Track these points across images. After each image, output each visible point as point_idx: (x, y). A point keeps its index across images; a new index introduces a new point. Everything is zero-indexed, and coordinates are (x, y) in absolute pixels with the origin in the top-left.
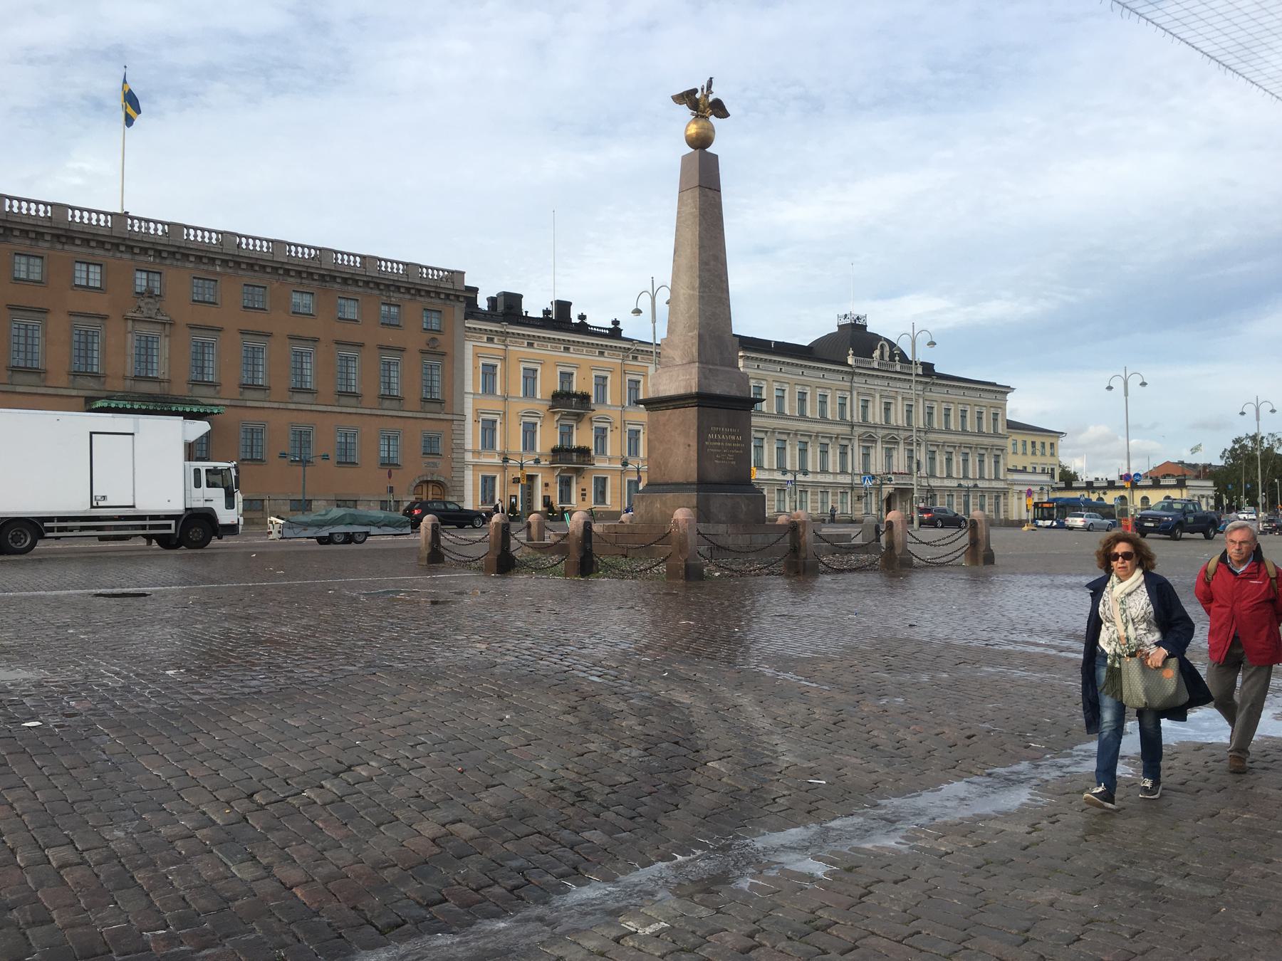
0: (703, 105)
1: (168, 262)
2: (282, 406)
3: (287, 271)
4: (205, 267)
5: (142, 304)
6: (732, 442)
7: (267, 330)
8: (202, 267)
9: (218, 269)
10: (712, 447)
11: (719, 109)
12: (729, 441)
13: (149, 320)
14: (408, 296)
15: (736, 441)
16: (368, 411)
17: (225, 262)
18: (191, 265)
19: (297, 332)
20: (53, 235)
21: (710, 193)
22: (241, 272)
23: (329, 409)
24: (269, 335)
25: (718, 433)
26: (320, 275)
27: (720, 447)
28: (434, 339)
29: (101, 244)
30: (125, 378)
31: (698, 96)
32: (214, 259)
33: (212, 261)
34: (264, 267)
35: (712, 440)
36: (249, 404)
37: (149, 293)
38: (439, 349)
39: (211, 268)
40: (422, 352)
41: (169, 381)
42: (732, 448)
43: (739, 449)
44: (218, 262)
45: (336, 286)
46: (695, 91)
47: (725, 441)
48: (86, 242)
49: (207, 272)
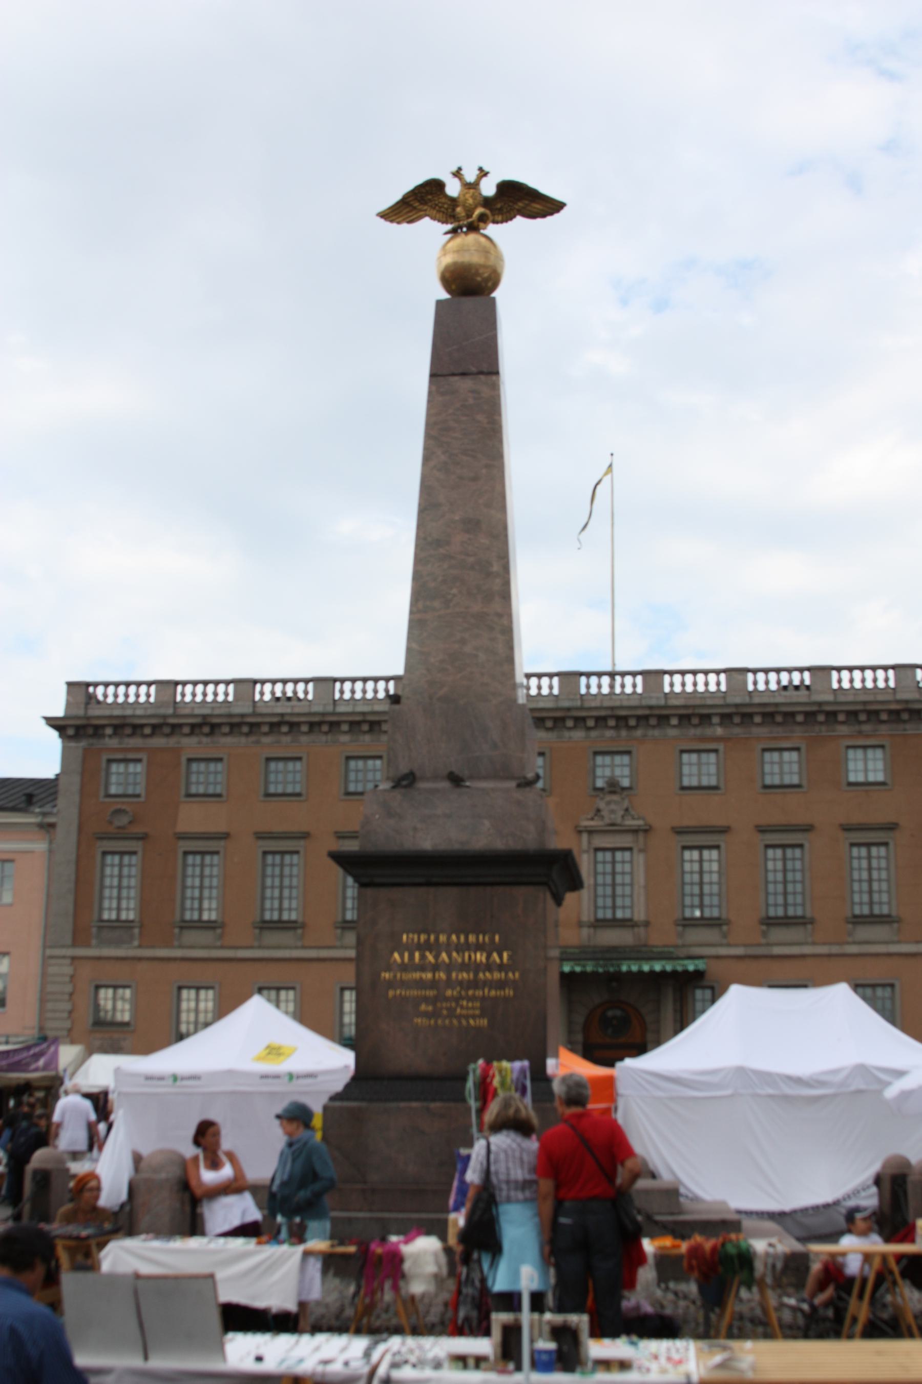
0: (477, 210)
1: (639, 733)
2: (835, 949)
4: (698, 731)
5: (602, 805)
6: (477, 968)
8: (692, 732)
9: (719, 731)
10: (404, 984)
12: (464, 967)
13: (613, 829)
15: (489, 967)
17: (726, 718)
19: (857, 818)
21: (464, 384)
24: (808, 829)
25: (424, 947)
26: (890, 712)
27: (433, 984)
30: (580, 924)
31: (453, 189)
33: (705, 719)
35: (404, 968)
36: (777, 950)
39: (708, 731)
41: (647, 924)
42: (475, 984)
43: (501, 985)
44: (716, 720)
46: (434, 187)
47: (449, 968)
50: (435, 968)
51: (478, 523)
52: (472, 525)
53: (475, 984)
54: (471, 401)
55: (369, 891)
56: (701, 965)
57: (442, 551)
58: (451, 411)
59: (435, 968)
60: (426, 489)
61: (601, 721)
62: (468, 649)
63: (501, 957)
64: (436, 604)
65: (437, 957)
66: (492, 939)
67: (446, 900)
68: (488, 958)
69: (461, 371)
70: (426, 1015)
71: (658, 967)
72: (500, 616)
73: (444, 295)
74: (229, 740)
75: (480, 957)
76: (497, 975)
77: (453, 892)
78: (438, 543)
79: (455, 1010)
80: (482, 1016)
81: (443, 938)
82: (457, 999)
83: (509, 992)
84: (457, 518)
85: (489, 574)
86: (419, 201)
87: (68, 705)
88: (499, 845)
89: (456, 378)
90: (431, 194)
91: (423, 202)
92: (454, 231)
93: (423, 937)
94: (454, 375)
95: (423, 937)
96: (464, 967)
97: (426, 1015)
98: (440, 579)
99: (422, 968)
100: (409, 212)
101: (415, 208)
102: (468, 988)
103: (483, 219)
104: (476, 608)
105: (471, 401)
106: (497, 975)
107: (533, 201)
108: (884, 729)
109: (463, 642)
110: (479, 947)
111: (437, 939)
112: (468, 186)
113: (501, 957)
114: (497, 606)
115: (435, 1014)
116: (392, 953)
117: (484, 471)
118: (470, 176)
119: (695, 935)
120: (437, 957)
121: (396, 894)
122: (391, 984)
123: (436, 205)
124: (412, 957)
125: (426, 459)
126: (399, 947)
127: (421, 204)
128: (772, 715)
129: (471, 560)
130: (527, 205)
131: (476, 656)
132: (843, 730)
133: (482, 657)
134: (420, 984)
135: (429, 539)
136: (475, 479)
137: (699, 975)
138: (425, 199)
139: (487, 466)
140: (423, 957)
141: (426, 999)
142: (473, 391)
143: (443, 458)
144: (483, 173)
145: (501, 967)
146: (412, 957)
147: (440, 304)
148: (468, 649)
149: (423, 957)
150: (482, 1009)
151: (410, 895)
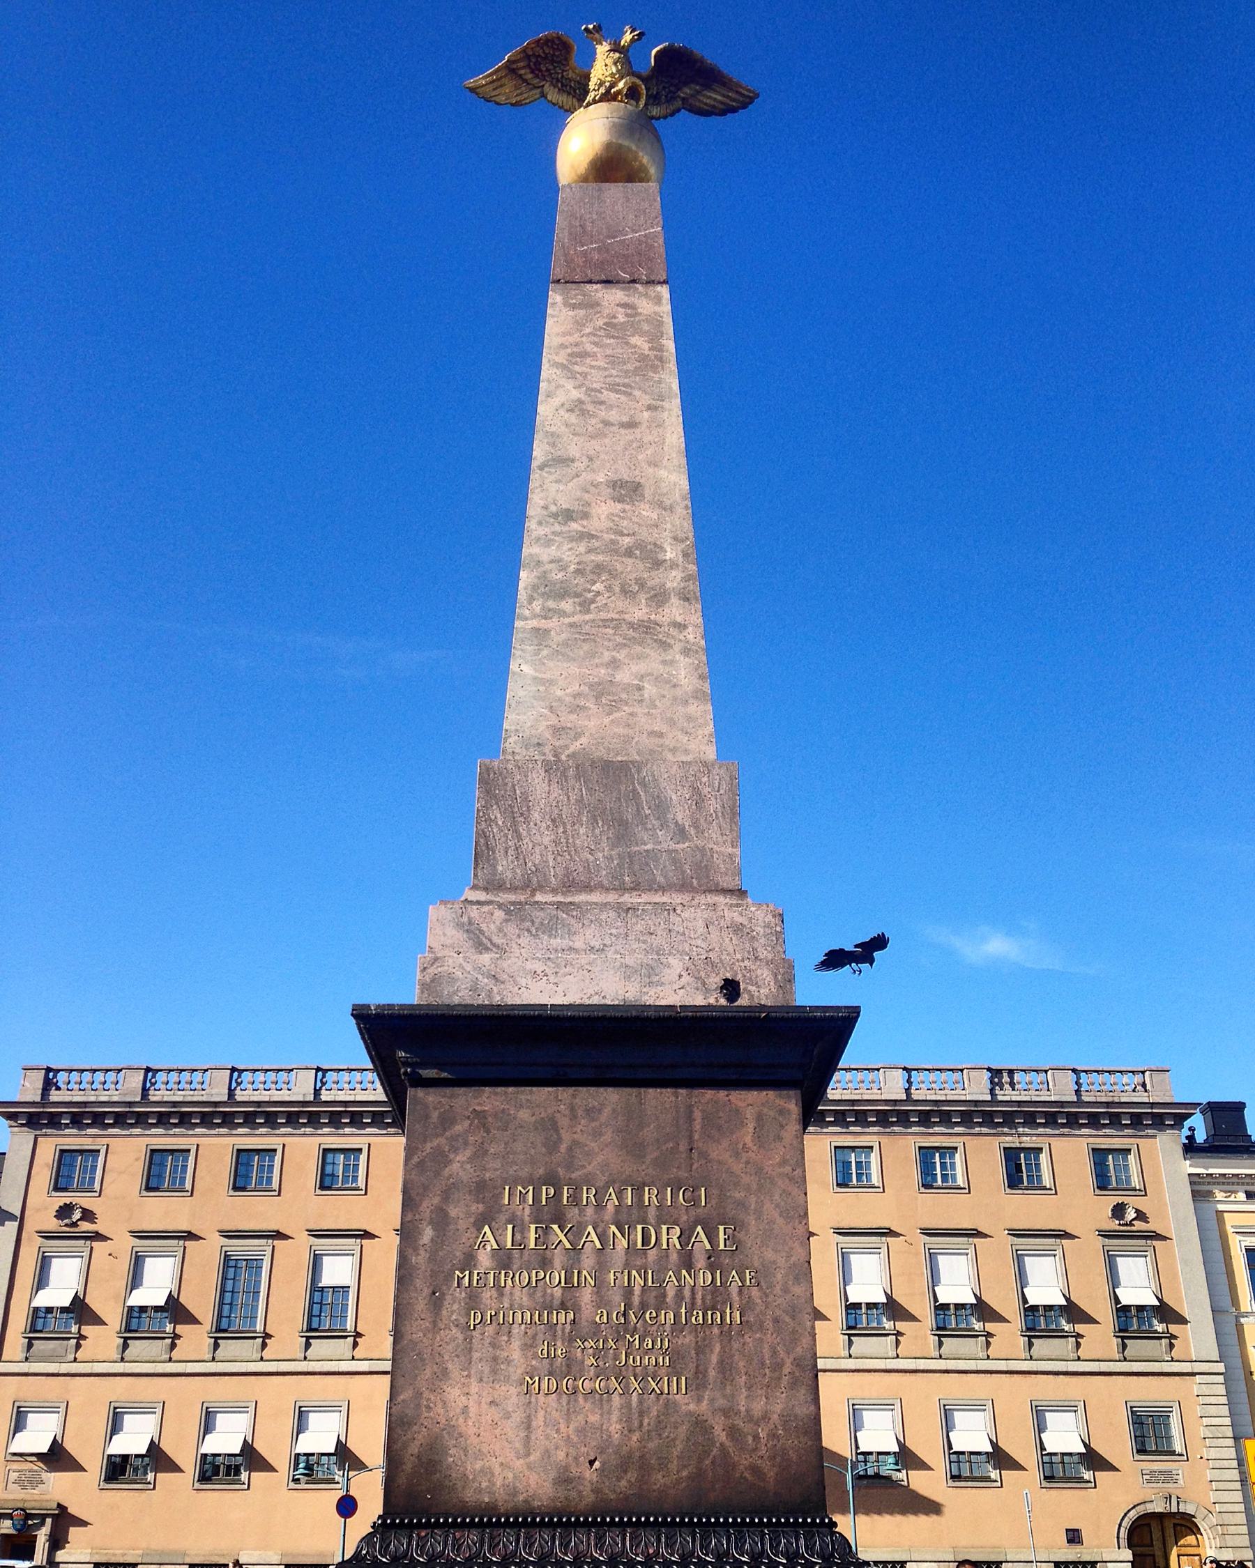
21: (611, 297)
35: (503, 1260)
54: (621, 318)
57: (574, 526)
58: (588, 331)
62: (623, 676)
63: (712, 1237)
64: (567, 605)
66: (695, 1202)
68: (685, 1236)
69: (604, 277)
76: (705, 1278)
77: (611, 1097)
78: (568, 515)
79: (616, 1357)
80: (675, 1370)
84: (601, 478)
85: (658, 564)
86: (532, 72)
89: (595, 286)
90: (552, 62)
93: (546, 1192)
94: (590, 282)
95: (546, 1192)
98: (572, 568)
100: (517, 88)
101: (525, 81)
102: (644, 1306)
104: (639, 612)
105: (621, 318)
106: (705, 1278)
107: (707, 87)
109: (614, 664)
111: (575, 1199)
113: (712, 1237)
116: (480, 1229)
117: (646, 414)
121: (490, 1099)
123: (558, 80)
127: (537, 76)
129: (626, 541)
130: (698, 92)
131: (640, 688)
133: (650, 690)
135: (553, 509)
136: (631, 425)
139: (649, 408)
142: (624, 305)
143: (576, 394)
148: (623, 676)
150: (676, 1356)
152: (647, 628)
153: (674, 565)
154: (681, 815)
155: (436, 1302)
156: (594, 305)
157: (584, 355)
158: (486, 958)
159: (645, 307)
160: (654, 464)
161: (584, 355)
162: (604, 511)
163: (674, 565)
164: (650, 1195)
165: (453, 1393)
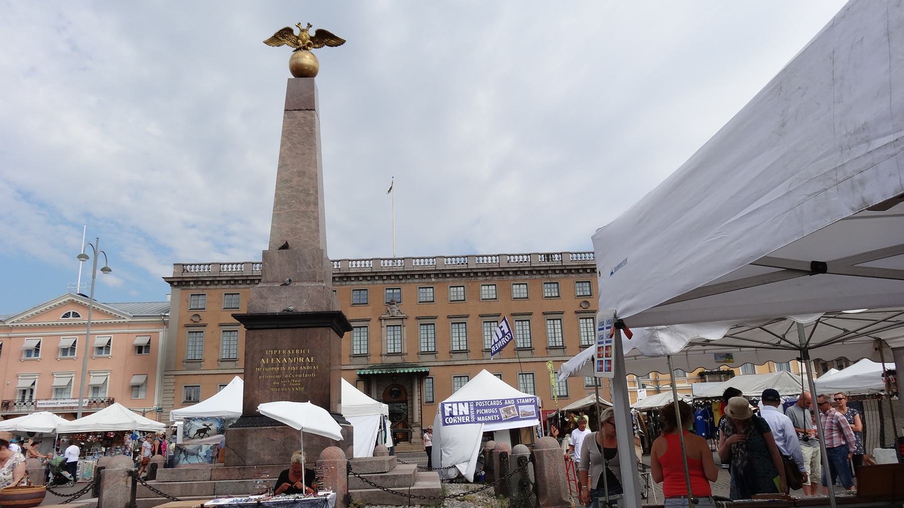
1: (403, 281)
2: (479, 362)
3: (476, 274)
4: (426, 280)
6: (300, 364)
7: (465, 313)
11: (324, 38)
12: (293, 364)
14: (563, 275)
15: (304, 364)
16: (540, 359)
17: (436, 275)
18: (417, 281)
20: (339, 278)
22: (447, 280)
23: (511, 361)
25: (276, 356)
28: (587, 302)
29: (365, 278)
31: (297, 32)
32: (429, 275)
34: (461, 273)
35: (266, 365)
36: (456, 363)
37: (392, 303)
38: (589, 309)
40: (576, 312)
42: (298, 372)
43: (310, 372)
45: (511, 278)
48: (357, 278)
49: (428, 283)
50: (281, 365)
51: (304, 173)
52: (301, 174)
53: (298, 372)
55: (251, 332)
56: (427, 369)
59: (281, 365)
60: (282, 158)
61: (389, 277)
62: (299, 226)
64: (285, 207)
65: (281, 360)
66: (306, 352)
67: (285, 336)
70: (276, 386)
71: (411, 371)
72: (313, 212)
73: (293, 77)
74: (242, 286)
75: (301, 360)
76: (308, 368)
78: (287, 181)
81: (284, 352)
82: (290, 379)
83: (314, 375)
85: (309, 194)
87: (174, 273)
88: (310, 310)
91: (283, 37)
92: (297, 50)
96: (293, 364)
97: (276, 386)
99: (275, 366)
103: (309, 45)
104: (303, 208)
106: (308, 368)
108: (495, 278)
109: (297, 223)
110: (301, 355)
112: (302, 31)
114: (312, 208)
115: (280, 386)
118: (304, 26)
119: (424, 358)
120: (281, 360)
122: (260, 373)
124: (270, 360)
125: (282, 146)
126: (264, 356)
128: (453, 274)
132: (481, 279)
134: (274, 373)
136: (304, 154)
137: (427, 373)
138: (283, 36)
140: (275, 360)
141: (276, 380)
144: (310, 26)
145: (310, 364)
146: (270, 360)
147: (289, 79)
148: (299, 226)
149: (275, 360)
151: (270, 334)
152: (305, 212)
153: (312, 195)
154: (310, 263)
155: (252, 374)
156: (296, 117)
157: (292, 133)
158: (262, 301)
159: (309, 117)
160: (309, 165)
161: (292, 133)
162: (296, 179)
163: (312, 195)
164: (297, 351)
165: (256, 392)
